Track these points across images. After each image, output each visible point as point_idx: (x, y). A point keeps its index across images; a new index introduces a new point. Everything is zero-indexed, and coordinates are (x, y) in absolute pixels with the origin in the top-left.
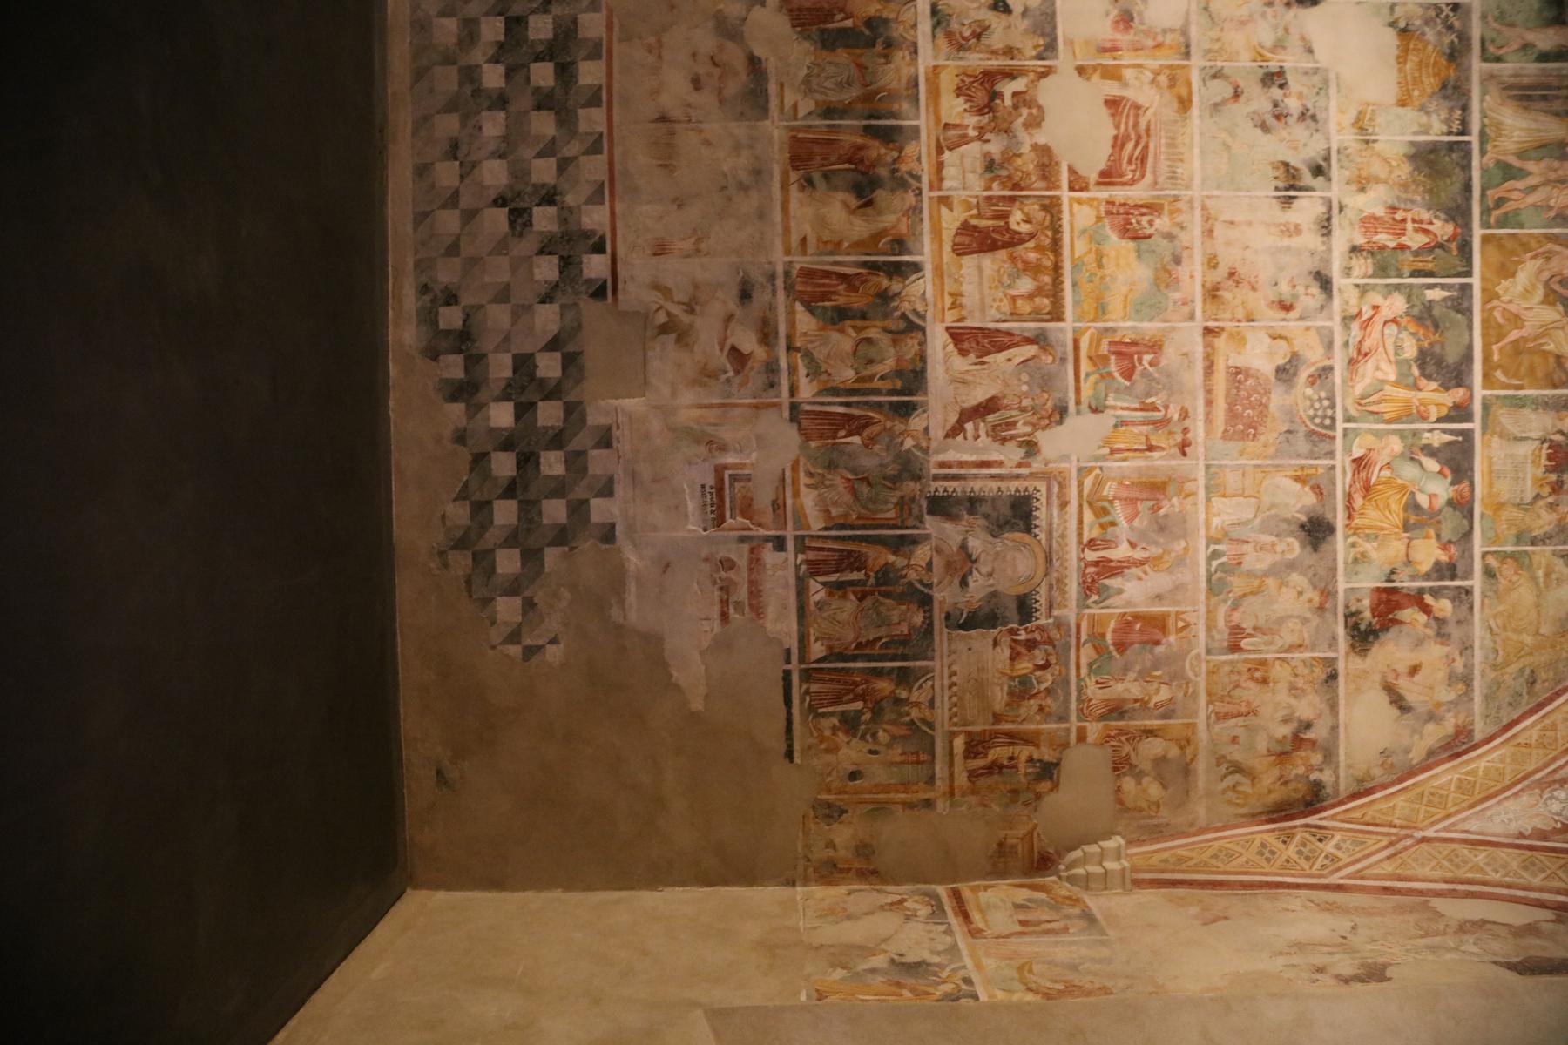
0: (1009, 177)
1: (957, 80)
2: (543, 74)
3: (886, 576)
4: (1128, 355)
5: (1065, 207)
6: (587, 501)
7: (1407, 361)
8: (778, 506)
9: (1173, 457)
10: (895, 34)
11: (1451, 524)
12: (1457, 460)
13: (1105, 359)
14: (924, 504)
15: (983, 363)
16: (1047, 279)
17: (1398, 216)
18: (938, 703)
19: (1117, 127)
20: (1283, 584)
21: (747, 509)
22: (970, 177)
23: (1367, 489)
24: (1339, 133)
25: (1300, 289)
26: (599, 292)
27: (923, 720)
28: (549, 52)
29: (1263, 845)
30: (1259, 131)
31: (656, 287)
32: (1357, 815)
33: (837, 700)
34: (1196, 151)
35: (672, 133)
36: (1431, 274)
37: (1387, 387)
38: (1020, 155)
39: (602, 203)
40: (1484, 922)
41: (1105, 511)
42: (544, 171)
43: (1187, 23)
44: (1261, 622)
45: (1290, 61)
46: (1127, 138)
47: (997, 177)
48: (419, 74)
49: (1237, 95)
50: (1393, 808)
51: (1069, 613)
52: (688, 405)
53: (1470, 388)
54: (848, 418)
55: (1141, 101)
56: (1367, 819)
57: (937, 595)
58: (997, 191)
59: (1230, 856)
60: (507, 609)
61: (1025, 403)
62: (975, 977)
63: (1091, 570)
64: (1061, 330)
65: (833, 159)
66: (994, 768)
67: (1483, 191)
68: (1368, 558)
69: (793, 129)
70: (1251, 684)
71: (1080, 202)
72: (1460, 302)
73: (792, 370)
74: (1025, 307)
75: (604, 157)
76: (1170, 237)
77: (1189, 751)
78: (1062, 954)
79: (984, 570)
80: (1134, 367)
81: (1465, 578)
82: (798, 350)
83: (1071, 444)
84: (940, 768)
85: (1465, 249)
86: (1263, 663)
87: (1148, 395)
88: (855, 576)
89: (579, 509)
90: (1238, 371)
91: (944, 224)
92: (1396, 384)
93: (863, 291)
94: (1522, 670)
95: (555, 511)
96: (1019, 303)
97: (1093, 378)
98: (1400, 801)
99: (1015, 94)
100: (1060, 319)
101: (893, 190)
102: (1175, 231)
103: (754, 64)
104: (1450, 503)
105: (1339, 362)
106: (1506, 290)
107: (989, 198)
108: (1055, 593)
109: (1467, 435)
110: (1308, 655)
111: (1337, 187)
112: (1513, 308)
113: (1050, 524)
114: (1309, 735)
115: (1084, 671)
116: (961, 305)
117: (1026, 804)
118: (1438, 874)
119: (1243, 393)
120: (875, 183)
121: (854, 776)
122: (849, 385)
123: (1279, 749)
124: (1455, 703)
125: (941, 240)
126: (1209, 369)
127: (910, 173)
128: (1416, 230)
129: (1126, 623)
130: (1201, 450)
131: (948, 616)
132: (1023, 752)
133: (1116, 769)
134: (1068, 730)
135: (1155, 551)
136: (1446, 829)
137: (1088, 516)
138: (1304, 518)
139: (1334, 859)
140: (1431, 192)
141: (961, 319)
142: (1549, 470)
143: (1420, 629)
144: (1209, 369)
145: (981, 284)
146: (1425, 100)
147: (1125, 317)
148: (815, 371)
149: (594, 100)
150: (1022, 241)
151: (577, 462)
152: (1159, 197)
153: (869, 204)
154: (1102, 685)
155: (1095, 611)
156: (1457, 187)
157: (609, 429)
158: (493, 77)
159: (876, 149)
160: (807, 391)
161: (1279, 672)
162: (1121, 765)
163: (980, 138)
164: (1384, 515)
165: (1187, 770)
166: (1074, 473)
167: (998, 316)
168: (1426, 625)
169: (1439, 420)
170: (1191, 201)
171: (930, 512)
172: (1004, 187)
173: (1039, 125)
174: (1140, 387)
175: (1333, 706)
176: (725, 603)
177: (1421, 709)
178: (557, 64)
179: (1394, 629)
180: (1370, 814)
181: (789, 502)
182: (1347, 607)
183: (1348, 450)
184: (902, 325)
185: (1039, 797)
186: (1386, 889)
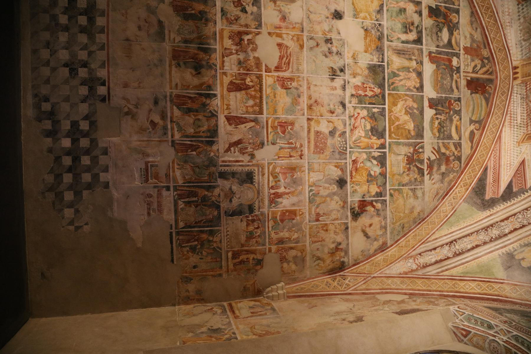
0: (246, 67)
1: (229, 34)
2: (83, 20)
3: (204, 199)
4: (284, 126)
5: (264, 78)
6: (99, 174)
7: (368, 130)
8: (167, 175)
9: (298, 159)
10: (209, 17)
11: (380, 180)
12: (382, 161)
13: (276, 127)
14: (217, 175)
15: (237, 128)
16: (258, 101)
17: (365, 86)
18: (223, 241)
19: (281, 53)
20: (332, 199)
21: (156, 177)
22: (233, 66)
23: (356, 169)
24: (348, 60)
25: (336, 107)
26: (103, 100)
27: (218, 247)
29: (327, 282)
30: (324, 57)
31: (124, 98)
32: (355, 271)
33: (189, 241)
34: (305, 62)
35: (131, 45)
36: (374, 104)
37: (362, 138)
38: (249, 60)
39: (105, 68)
40: (390, 301)
41: (276, 177)
42: (83, 55)
43: (303, 21)
44: (325, 212)
45: (334, 36)
47: (242, 67)
49: (318, 45)
50: (365, 268)
51: (265, 210)
52: (135, 140)
53: (385, 139)
54: (192, 145)
55: (288, 45)
56: (358, 272)
57: (222, 205)
58: (242, 71)
59: (317, 286)
61: (251, 141)
62: (236, 332)
63: (272, 196)
64: (262, 117)
65: (187, 57)
66: (242, 262)
67: (388, 80)
68: (356, 192)
69: (173, 46)
70: (322, 232)
71: (268, 76)
72: (382, 113)
73: (172, 129)
74: (250, 110)
75: (106, 52)
76: (297, 89)
77: (304, 253)
78: (264, 322)
79: (237, 196)
80: (285, 130)
81: (384, 197)
82: (174, 122)
83: (266, 155)
84: (224, 263)
86: (326, 224)
87: (290, 139)
88: (196, 199)
89: (96, 177)
90: (318, 132)
91: (224, 81)
92: (365, 137)
93: (197, 103)
94: (400, 224)
95: (87, 177)
96: (249, 108)
97: (272, 134)
98: (367, 266)
99: (248, 40)
100: (262, 114)
101: (207, 69)
102: (299, 87)
103: (160, 23)
104: (380, 174)
106: (395, 110)
107: (239, 73)
108: (261, 204)
109: (385, 153)
110: (339, 222)
111: (347, 77)
112: (397, 115)
113: (259, 181)
114: (340, 247)
115: (270, 229)
116: (230, 109)
117: (253, 273)
118: (378, 287)
119: (319, 139)
120: (201, 67)
121: (195, 267)
122: (192, 134)
123: (331, 252)
124: (382, 235)
125: (223, 86)
126: (309, 131)
127: (213, 64)
128: (370, 90)
129: (283, 213)
130: (306, 157)
131: (226, 212)
132: (251, 256)
133: (281, 261)
134: (266, 248)
135: (292, 189)
136: (380, 274)
137: (271, 178)
138: (338, 179)
139: (348, 285)
140: (374, 79)
141: (230, 113)
142: (407, 164)
143: (372, 213)
144: (309, 131)
145: (236, 102)
146: (372, 51)
147: (283, 114)
148: (180, 129)
149: (102, 31)
150: (250, 88)
151: (95, 160)
152: (293, 76)
153: (199, 73)
154: (276, 233)
155: (274, 209)
156: (381, 78)
157: (107, 148)
158: (63, 20)
159: (202, 55)
160: (177, 136)
161: (331, 227)
162: (283, 259)
163: (236, 53)
164: (361, 177)
165: (303, 260)
166: (266, 164)
167: (242, 112)
168: (374, 211)
169: (377, 149)
170: (303, 78)
171: (220, 177)
172: (244, 70)
173: (256, 50)
174: (287, 137)
175: (347, 237)
176: (149, 209)
177: (373, 237)
178: (88, 17)
179: (365, 213)
180: (359, 270)
181: (171, 174)
182: (351, 206)
183: (351, 157)
184: (210, 114)
185: (257, 271)
186: (363, 293)
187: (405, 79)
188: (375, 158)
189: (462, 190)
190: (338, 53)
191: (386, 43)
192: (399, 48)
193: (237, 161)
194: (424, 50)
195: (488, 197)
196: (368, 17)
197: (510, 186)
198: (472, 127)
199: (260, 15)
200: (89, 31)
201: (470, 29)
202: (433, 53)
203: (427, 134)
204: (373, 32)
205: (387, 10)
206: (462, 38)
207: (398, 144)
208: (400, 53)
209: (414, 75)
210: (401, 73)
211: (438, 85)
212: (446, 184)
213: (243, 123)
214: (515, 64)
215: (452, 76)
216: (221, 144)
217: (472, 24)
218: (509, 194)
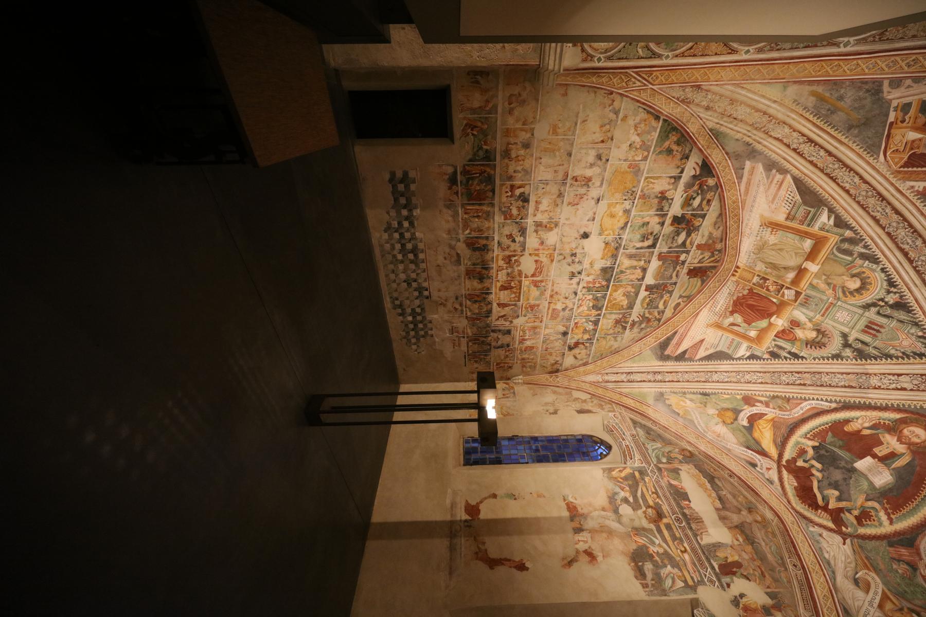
2: (411, 256)
3: (483, 342)
4: (532, 307)
8: (463, 332)
12: (596, 323)
26: (427, 298)
28: (412, 251)
42: (413, 276)
45: (578, 251)
48: (383, 256)
52: (446, 317)
60: (414, 347)
72: (604, 297)
78: (508, 404)
85: (608, 287)
89: (426, 333)
93: (481, 297)
103: (458, 254)
105: (575, 307)
111: (583, 276)
148: (470, 310)
149: (423, 262)
151: (425, 325)
158: (400, 257)
159: (484, 271)
160: (469, 314)
162: (523, 366)
165: (535, 367)
189: (653, 340)
190: (580, 262)
191: (621, 250)
195: (666, 353)
197: (685, 352)
198: (680, 300)
199: (524, 243)
200: (415, 262)
201: (711, 229)
209: (639, 271)
211: (659, 274)
212: (642, 334)
214: (739, 264)
215: (675, 268)
216: (494, 315)
218: (681, 357)
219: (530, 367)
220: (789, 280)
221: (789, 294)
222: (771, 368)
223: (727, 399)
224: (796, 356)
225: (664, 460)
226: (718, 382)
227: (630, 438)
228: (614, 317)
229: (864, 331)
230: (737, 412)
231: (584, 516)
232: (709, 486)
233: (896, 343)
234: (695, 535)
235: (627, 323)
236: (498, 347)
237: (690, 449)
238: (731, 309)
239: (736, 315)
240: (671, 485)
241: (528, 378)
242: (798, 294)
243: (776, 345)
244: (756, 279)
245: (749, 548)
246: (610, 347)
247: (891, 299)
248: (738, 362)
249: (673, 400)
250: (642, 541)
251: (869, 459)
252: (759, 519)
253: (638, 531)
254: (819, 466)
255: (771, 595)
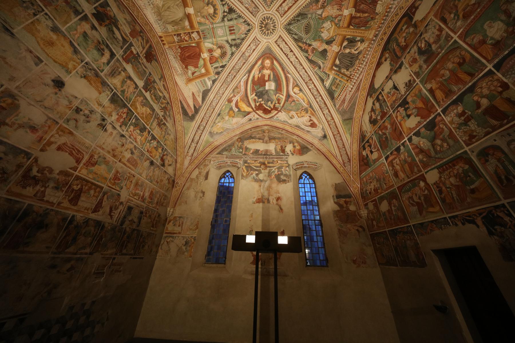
0: (63, 185)
4: (116, 178)
12: (154, 138)
13: (115, 183)
16: (93, 187)
19: (67, 152)
22: (56, 195)
24: (99, 110)
34: (84, 139)
36: (131, 119)
38: (58, 179)
45: (76, 103)
46: (71, 152)
49: (76, 121)
51: (145, 205)
57: (134, 228)
58: (65, 189)
66: (156, 223)
71: (80, 171)
72: (137, 119)
73: (81, 254)
76: (100, 157)
83: (124, 195)
98: (178, 172)
99: (38, 172)
102: (99, 155)
105: (135, 144)
107: (66, 192)
109: (152, 134)
125: (70, 208)
137: (135, 197)
140: (119, 106)
147: (110, 175)
150: (82, 189)
161: (162, 178)
162: (162, 205)
163: (46, 188)
165: (166, 196)
173: (53, 170)
174: (122, 178)
181: (108, 256)
187: (128, 88)
188: (151, 140)
191: (102, 74)
192: (110, 71)
193: (119, 213)
194: (119, 58)
195: (190, 115)
196: (75, 63)
197: (195, 107)
198: (162, 82)
202: (124, 55)
203: (155, 106)
204: (90, 74)
205: (78, 45)
206: (124, 26)
207: (152, 124)
208: (113, 75)
209: (129, 81)
210: (124, 88)
212: (172, 118)
213: (102, 202)
214: (160, 34)
215: (139, 62)
217: (120, 9)
218: (197, 111)
219: (164, 199)
220: (188, 27)
221: (195, 35)
222: (222, 80)
223: (225, 108)
224: (223, 67)
225: (241, 150)
226: (217, 105)
227: (228, 160)
228: (155, 124)
229: (231, 34)
230: (231, 109)
231: (263, 196)
232: (253, 140)
233: (241, 31)
234: (272, 155)
235: (162, 121)
236: (139, 222)
237: (237, 138)
238: (184, 67)
239: (189, 67)
240: (252, 153)
241: (171, 204)
242: (198, 32)
243: (215, 68)
244: (176, 38)
245: (277, 140)
246: (172, 140)
247: (227, 10)
248: (213, 89)
249: (215, 130)
250: (273, 176)
251: (267, 83)
252: (267, 131)
253: (269, 175)
254: (261, 100)
255: (290, 143)
